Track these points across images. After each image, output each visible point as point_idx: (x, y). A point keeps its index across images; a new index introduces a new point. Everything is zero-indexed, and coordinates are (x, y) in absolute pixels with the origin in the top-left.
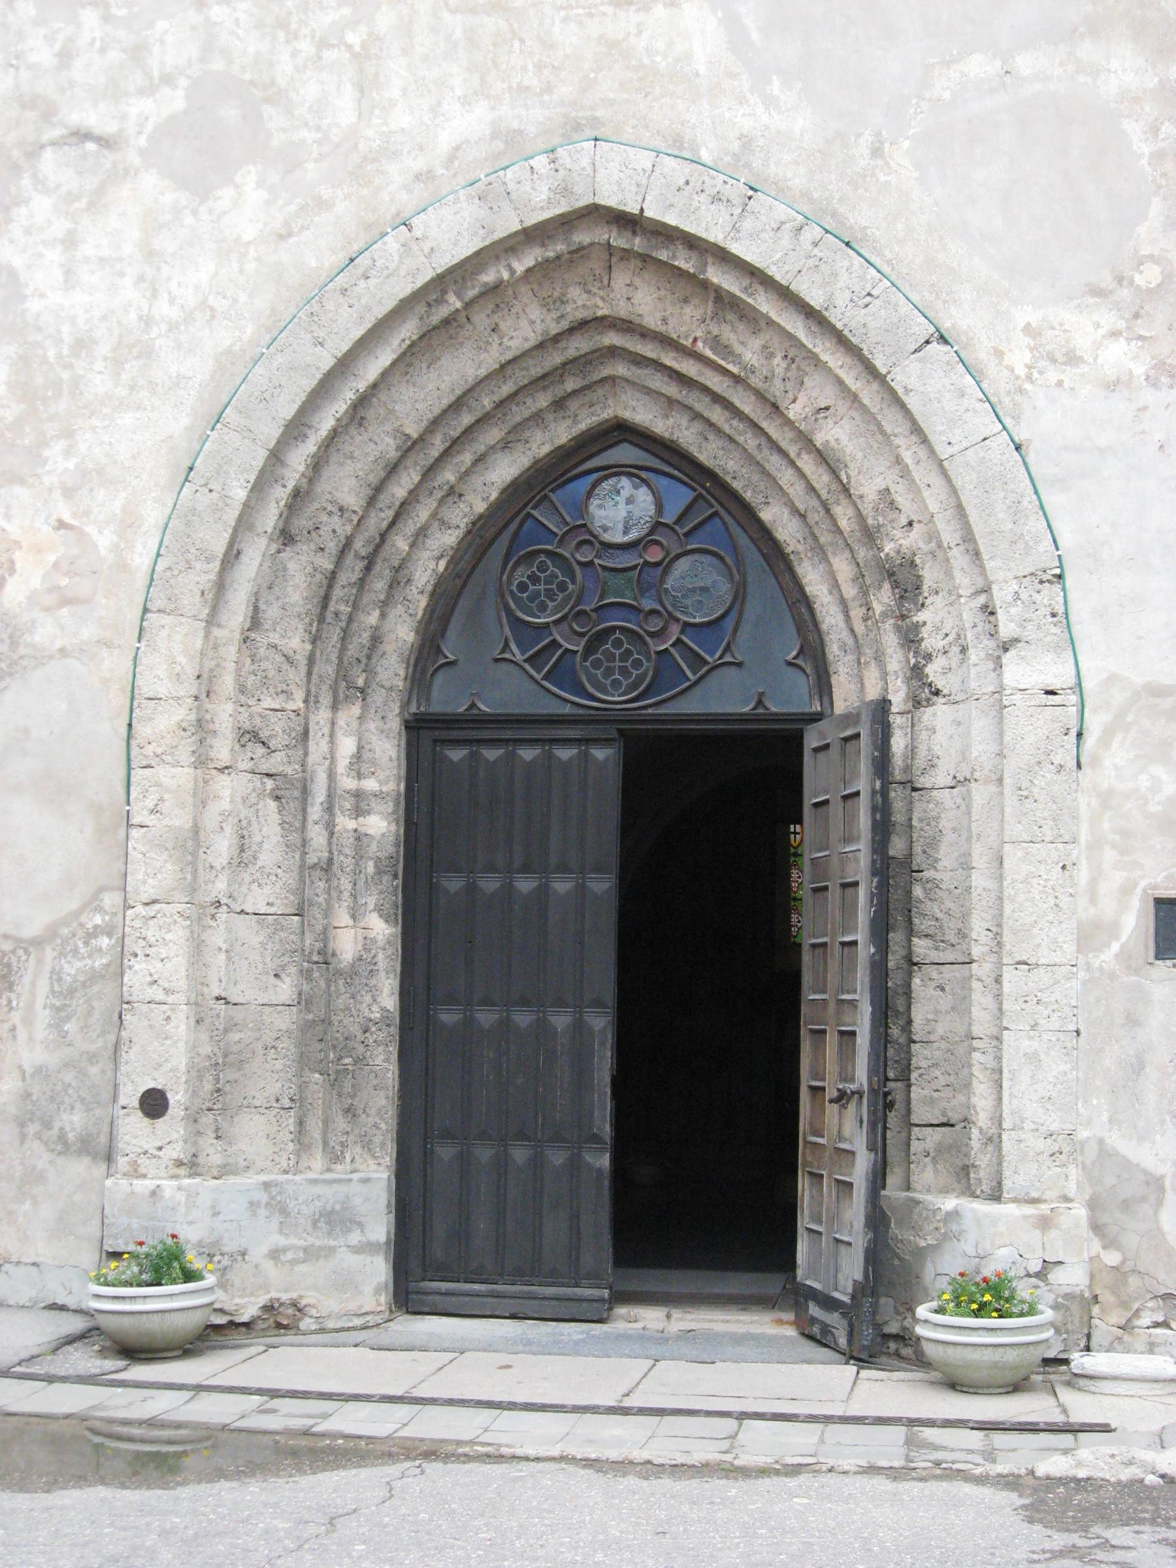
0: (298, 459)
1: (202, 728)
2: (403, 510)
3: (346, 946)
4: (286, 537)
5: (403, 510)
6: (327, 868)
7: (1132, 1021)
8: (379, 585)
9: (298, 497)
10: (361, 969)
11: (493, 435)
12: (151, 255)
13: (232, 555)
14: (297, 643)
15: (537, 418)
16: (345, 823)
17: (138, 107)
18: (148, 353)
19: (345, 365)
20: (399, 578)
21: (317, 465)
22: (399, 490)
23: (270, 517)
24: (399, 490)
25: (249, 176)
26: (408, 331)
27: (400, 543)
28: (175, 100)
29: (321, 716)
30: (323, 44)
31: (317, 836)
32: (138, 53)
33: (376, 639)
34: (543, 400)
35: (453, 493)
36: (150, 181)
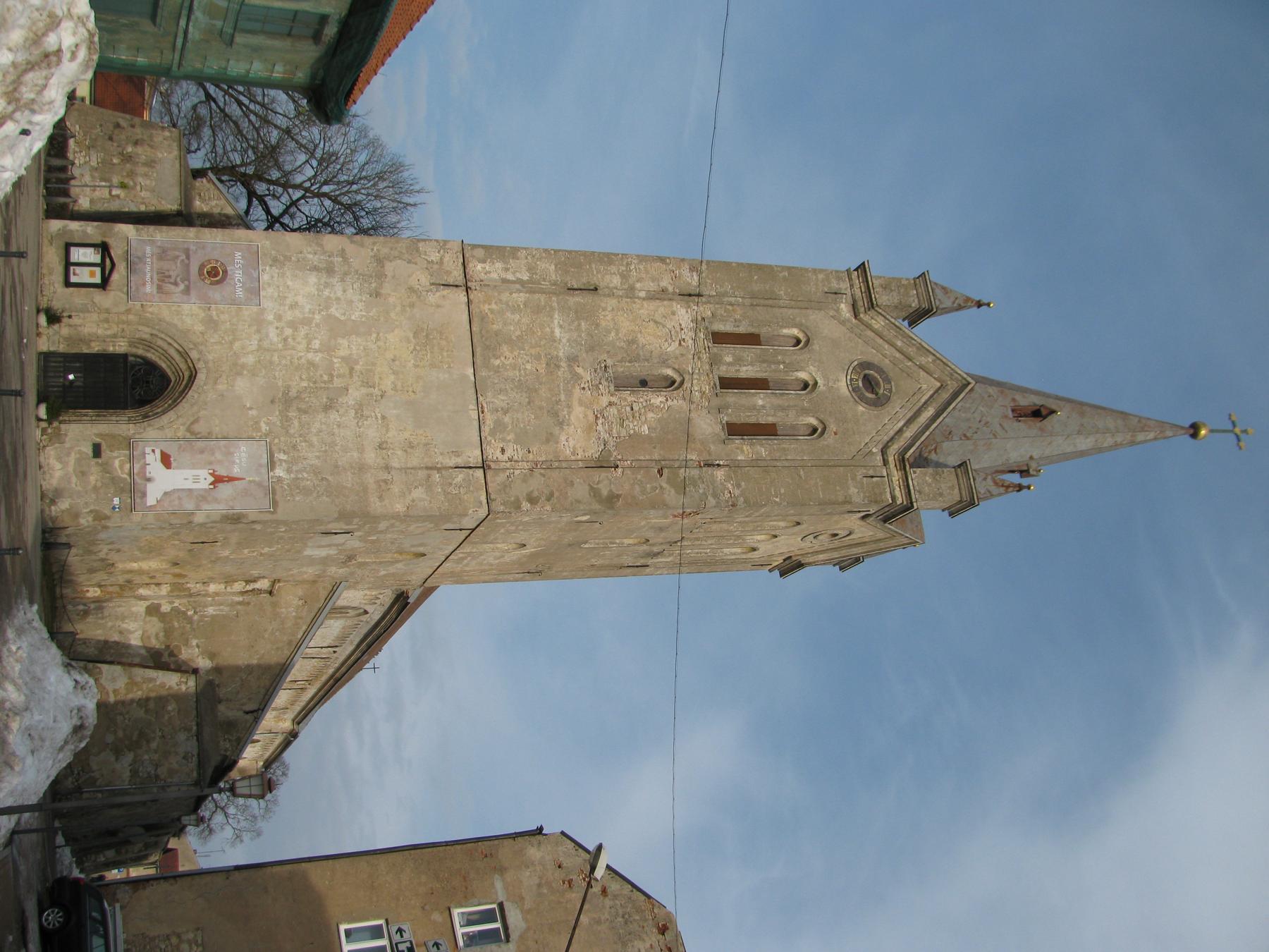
0: (163, 336)
1: (124, 322)
2: (157, 351)
3: (93, 344)
4: (152, 335)
5: (157, 351)
6: (104, 341)
7: (84, 440)
8: (147, 348)
9: (156, 336)
10: (89, 347)
11: (169, 363)
12: (192, 316)
13: (148, 327)
14: (137, 336)
15: (171, 370)
16: (111, 344)
17: (214, 313)
18: (177, 315)
19: (175, 341)
20: (148, 351)
21: (162, 339)
22: (160, 350)
23: (154, 332)
24: (160, 350)
25: (203, 328)
26: (181, 349)
27: (153, 351)
28: (216, 318)
29: (125, 340)
30: (223, 338)
31: (108, 340)
32: (223, 313)
33: (138, 348)
34: (174, 370)
35: (160, 358)
36: (203, 315)
